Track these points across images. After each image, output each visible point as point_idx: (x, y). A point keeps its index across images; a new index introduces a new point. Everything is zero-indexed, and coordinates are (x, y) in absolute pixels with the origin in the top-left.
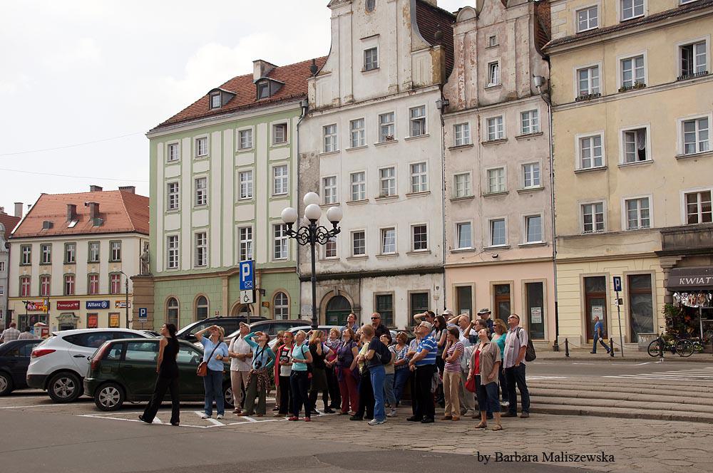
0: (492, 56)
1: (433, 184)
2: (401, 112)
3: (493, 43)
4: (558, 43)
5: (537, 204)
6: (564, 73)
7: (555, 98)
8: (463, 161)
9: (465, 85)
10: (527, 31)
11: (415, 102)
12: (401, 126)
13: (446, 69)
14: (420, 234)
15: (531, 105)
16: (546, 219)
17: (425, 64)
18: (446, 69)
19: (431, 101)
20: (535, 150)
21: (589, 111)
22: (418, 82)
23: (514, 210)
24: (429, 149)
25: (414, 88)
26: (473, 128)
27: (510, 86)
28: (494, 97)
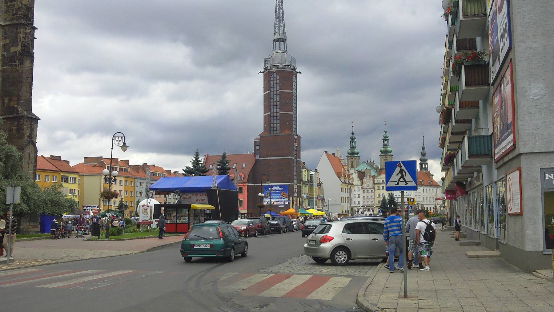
0: (368, 183)
1: (361, 196)
2: (356, 188)
3: (368, 182)
4: (375, 183)
5: (373, 200)
6: (376, 187)
7: (375, 189)
8: (364, 195)
9: (365, 186)
10: (372, 181)
11: (358, 187)
12: (356, 189)
13: (362, 184)
14: (359, 202)
15: (372, 189)
16: (374, 202)
17: (360, 183)
18: (362, 184)
19: (360, 187)
20: (373, 194)
21: (379, 190)
22: (359, 184)
23: (370, 201)
24: (360, 193)
25: (358, 185)
26: (366, 191)
27: (370, 187)
28: (368, 188)
